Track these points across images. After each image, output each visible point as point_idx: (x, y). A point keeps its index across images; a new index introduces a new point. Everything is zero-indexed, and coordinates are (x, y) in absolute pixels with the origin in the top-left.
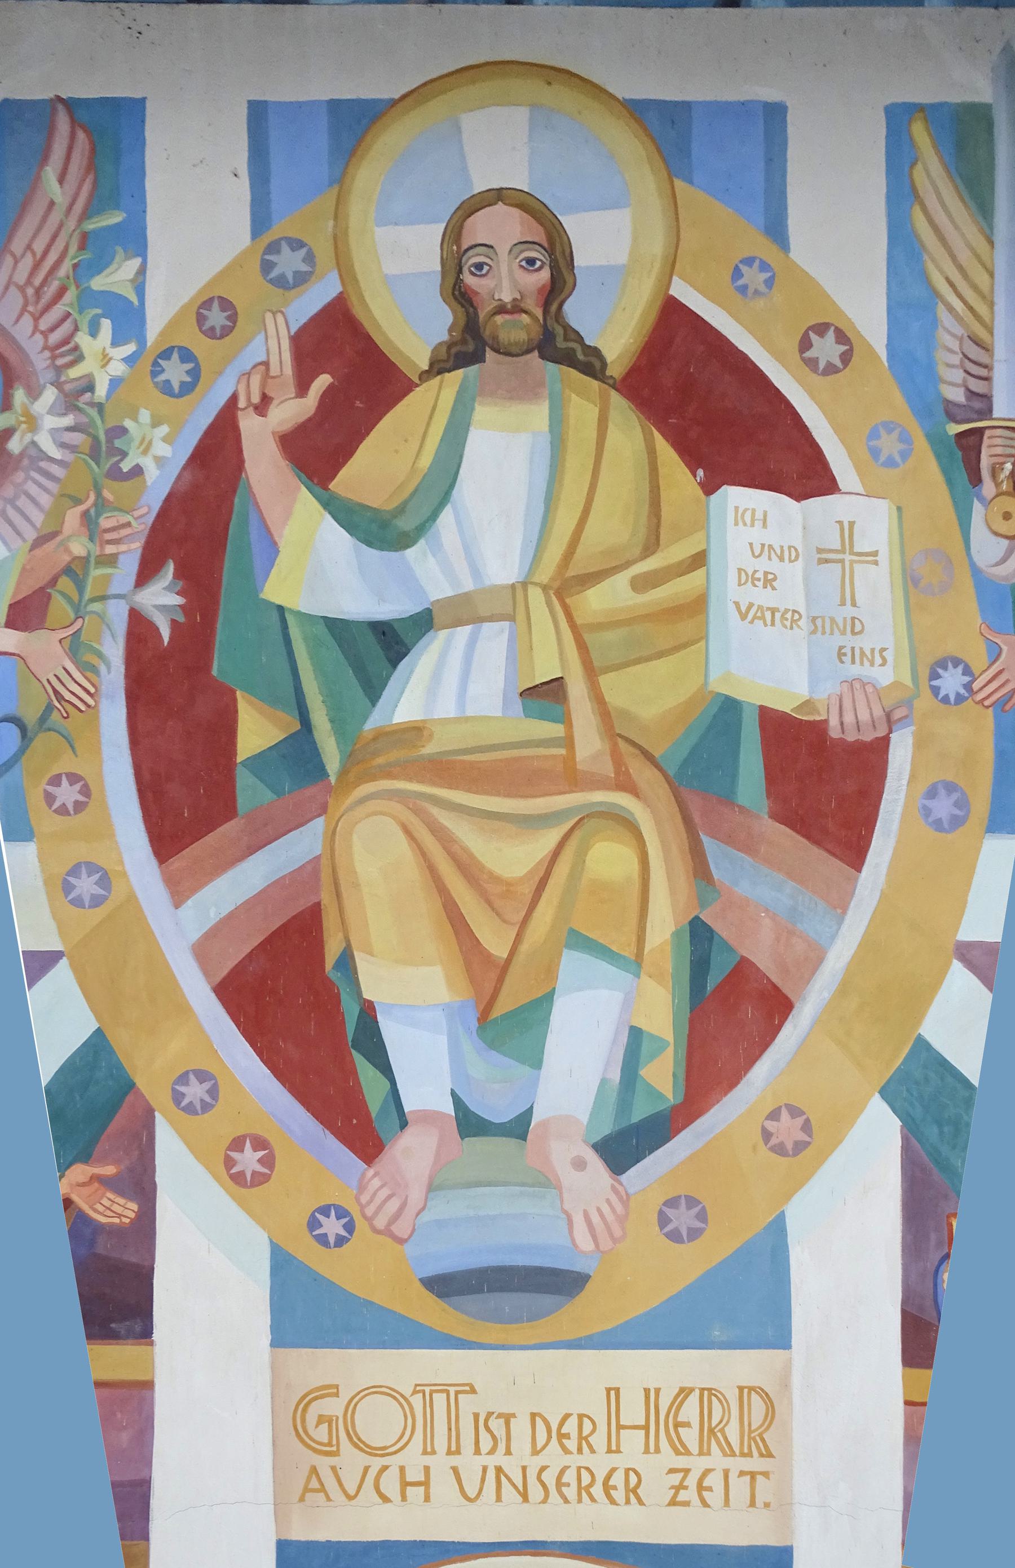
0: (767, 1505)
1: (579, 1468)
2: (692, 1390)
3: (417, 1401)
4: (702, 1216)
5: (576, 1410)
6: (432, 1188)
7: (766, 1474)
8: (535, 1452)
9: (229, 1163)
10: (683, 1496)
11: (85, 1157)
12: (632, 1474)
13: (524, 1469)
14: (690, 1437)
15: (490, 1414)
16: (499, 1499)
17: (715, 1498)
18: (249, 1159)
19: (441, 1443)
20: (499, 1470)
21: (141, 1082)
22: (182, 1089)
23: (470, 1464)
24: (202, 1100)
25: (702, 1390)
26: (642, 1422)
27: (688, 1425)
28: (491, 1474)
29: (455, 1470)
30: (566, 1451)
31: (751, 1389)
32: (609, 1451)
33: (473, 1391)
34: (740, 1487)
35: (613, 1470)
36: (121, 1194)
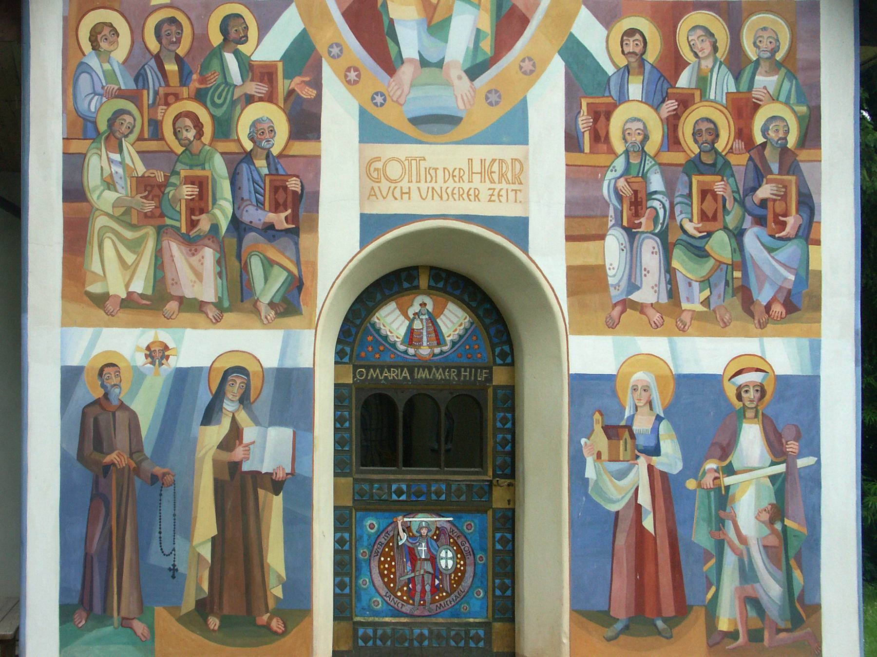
0: (520, 202)
1: (459, 188)
2: (496, 160)
3: (406, 163)
4: (499, 97)
5: (458, 167)
6: (412, 86)
7: (520, 190)
8: (445, 182)
9: (346, 76)
10: (493, 198)
11: (299, 75)
12: (476, 190)
13: (441, 188)
14: (495, 177)
15: (430, 168)
16: (433, 199)
17: (503, 199)
18: (352, 75)
19: (414, 179)
20: (433, 188)
21: (318, 47)
22: (331, 49)
23: (423, 186)
24: (338, 54)
25: (500, 160)
26: (480, 171)
27: (494, 172)
28: (430, 190)
29: (419, 188)
30: (455, 182)
31: (516, 159)
32: (469, 182)
33: (425, 159)
34: (512, 195)
35: (470, 189)
36: (311, 87)
